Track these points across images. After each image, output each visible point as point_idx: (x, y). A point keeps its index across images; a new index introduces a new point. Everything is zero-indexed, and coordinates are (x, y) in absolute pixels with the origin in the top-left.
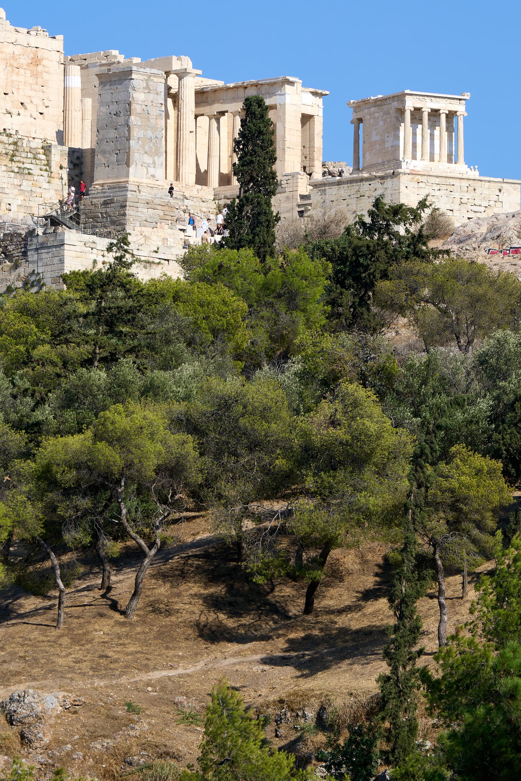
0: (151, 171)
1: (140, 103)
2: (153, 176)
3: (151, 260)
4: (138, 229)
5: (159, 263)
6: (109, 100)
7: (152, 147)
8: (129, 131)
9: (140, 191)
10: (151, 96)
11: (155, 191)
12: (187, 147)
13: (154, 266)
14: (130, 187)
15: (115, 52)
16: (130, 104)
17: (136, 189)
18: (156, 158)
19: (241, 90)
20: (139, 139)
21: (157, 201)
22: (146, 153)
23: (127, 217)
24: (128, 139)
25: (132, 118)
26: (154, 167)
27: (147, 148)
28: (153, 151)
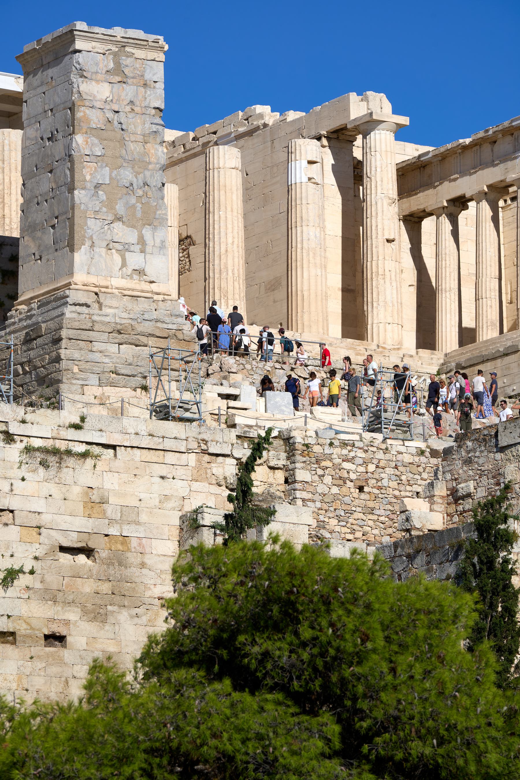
0: (135, 260)
1: (98, 104)
2: (140, 272)
3: (62, 446)
4: (93, 391)
5: (85, 455)
6: (40, 110)
7: (134, 206)
8: (72, 170)
9: (100, 305)
10: (129, 92)
11: (143, 305)
12: (381, 272)
13: (71, 461)
14: (73, 296)
15: (259, 109)
16: (72, 109)
17: (90, 299)
18: (147, 233)
19: (487, 148)
20: (97, 186)
21: (147, 327)
22: (119, 219)
23: (64, 364)
24: (71, 189)
25: (79, 139)
26: (143, 251)
27: (120, 208)
28: (139, 214)
